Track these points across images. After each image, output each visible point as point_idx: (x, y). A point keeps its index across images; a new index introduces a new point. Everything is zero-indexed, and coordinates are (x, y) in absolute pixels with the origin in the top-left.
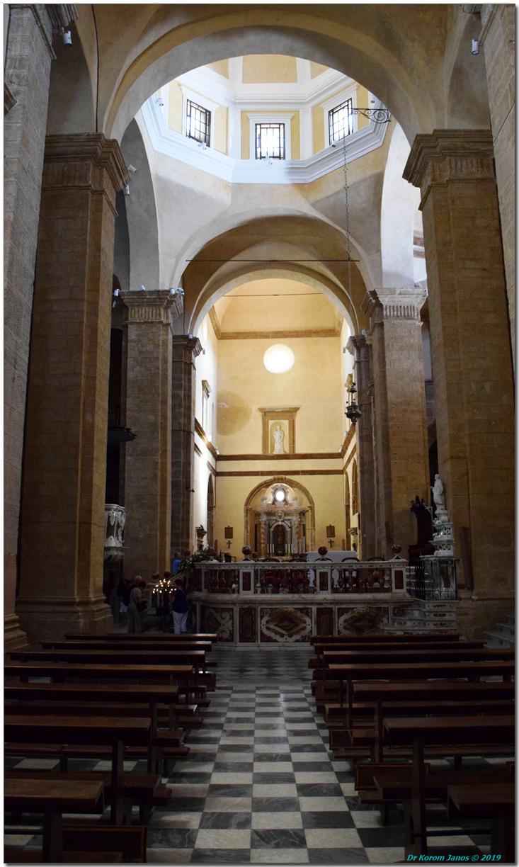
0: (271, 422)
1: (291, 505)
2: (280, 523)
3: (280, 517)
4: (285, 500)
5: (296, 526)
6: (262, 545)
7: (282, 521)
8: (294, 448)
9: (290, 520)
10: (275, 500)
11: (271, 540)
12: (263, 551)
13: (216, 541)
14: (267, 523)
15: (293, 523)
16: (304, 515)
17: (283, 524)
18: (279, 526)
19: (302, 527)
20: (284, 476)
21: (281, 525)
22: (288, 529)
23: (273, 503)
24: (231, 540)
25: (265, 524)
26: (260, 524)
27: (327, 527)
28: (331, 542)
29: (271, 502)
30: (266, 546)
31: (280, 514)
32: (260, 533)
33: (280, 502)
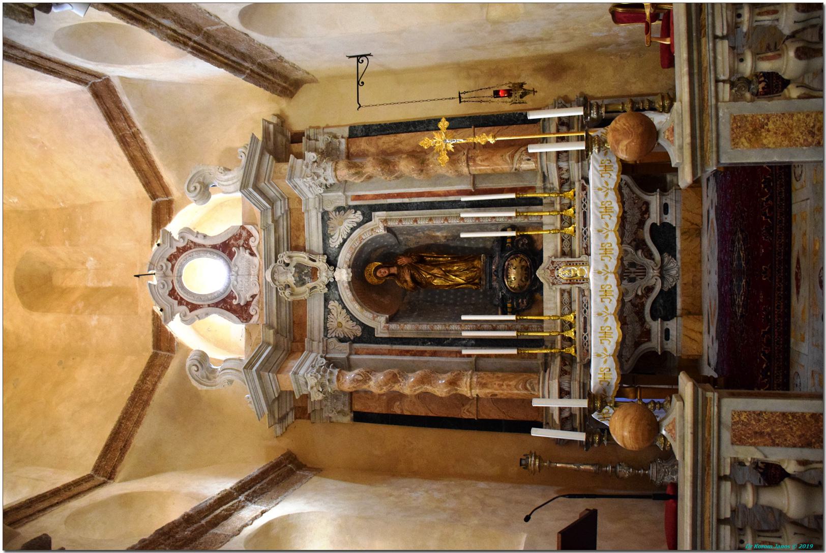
2: (343, 275)
3: (305, 274)
5: (344, 173)
6: (464, 389)
7: (332, 263)
9: (325, 217)
11: (438, 328)
12: (511, 389)
14: (340, 352)
15: (338, 198)
17: (345, 257)
18: (359, 283)
19: (363, 144)
21: (359, 266)
22: (377, 226)
23: (242, 312)
25: (345, 365)
30: (477, 365)
31: (290, 279)
32: (424, 397)
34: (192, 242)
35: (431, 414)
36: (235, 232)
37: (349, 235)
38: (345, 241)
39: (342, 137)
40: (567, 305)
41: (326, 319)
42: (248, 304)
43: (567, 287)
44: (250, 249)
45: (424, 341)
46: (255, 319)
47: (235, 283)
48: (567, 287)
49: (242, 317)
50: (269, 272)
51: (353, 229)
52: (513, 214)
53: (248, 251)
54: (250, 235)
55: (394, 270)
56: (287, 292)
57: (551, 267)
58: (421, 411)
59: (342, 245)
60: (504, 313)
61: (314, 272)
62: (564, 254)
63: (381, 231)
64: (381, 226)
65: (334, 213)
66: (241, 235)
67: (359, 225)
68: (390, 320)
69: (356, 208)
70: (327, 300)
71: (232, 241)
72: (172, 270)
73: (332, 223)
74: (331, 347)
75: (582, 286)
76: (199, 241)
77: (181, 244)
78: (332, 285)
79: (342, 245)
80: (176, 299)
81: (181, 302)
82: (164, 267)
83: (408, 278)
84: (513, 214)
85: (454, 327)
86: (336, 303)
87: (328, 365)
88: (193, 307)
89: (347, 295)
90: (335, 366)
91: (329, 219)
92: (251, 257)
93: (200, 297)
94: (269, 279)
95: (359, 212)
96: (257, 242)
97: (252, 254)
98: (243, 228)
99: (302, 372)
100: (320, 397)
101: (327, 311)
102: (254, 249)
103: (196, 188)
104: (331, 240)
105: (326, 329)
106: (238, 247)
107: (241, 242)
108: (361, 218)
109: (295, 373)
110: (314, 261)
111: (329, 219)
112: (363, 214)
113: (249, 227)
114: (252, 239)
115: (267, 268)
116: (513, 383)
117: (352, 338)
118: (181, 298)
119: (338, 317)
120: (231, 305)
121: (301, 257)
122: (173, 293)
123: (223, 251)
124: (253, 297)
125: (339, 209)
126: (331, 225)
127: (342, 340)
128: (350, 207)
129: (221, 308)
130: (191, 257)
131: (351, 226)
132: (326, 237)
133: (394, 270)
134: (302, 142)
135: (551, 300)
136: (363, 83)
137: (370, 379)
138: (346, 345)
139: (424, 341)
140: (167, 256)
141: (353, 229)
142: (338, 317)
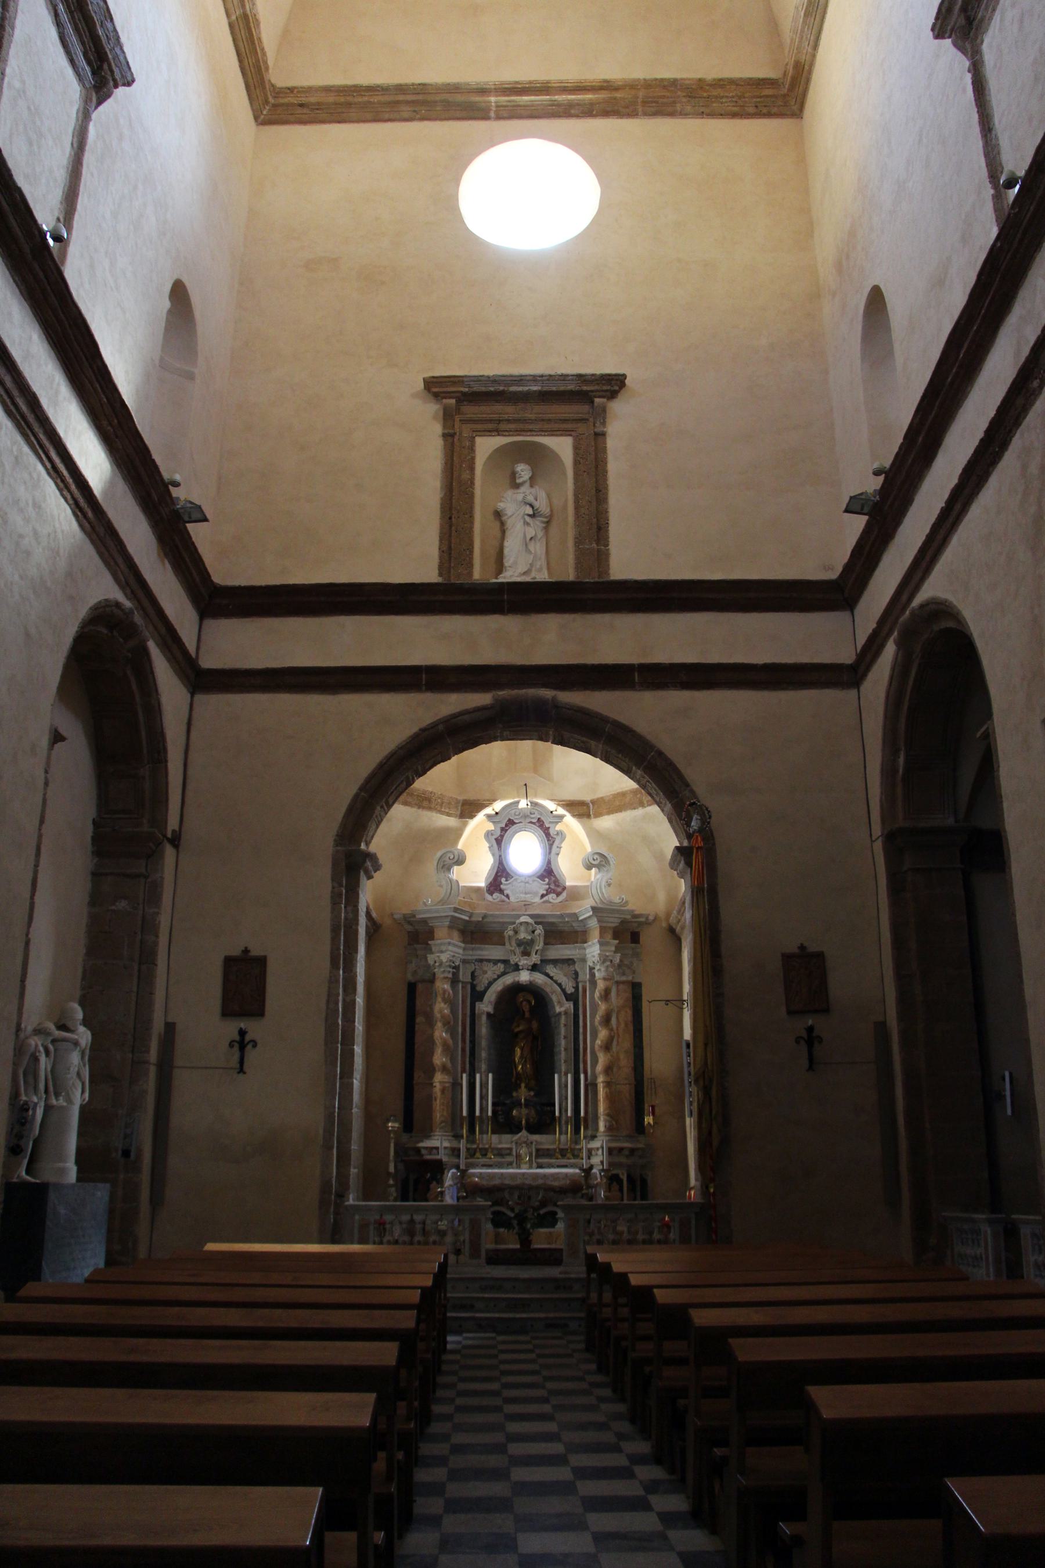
0: (486, 446)
1: (576, 894)
2: (524, 977)
3: (526, 947)
4: (548, 873)
5: (601, 985)
8: (602, 557)
9: (570, 962)
10: (501, 874)
12: (439, 1111)
13: (170, 1028)
14: (464, 976)
15: (584, 976)
16: (635, 938)
17: (539, 978)
18: (517, 988)
20: (547, 693)
22: (561, 1007)
24: (254, 1028)
25: (454, 981)
26: (432, 980)
27: (787, 958)
28: (811, 1039)
29: (482, 884)
30: (456, 1085)
31: (523, 935)
33: (527, 879)
34: (553, 842)
35: (416, 1046)
36: (561, 881)
37: (556, 982)
38: (551, 978)
39: (633, 977)
40: (500, 1153)
41: (489, 961)
42: (501, 891)
43: (514, 1153)
44: (547, 895)
45: (473, 1042)
46: (489, 897)
47: (519, 881)
48: (514, 1153)
49: (491, 887)
50: (529, 920)
51: (560, 985)
52: (569, 1114)
53: (545, 892)
54: (558, 894)
55: (527, 1015)
56: (511, 933)
57: (529, 1142)
58: (419, 1039)
59: (547, 975)
60: (494, 1104)
61: (526, 953)
62: (538, 1150)
63: (558, 1009)
64: (563, 1009)
65: (573, 969)
66: (558, 886)
67: (564, 991)
68: (489, 1015)
69: (577, 988)
70: (505, 962)
71: (553, 879)
72: (531, 822)
73: (565, 966)
74: (468, 966)
75: (514, 1164)
76: (554, 847)
77: (551, 831)
78: (517, 968)
79: (547, 975)
80: (506, 825)
81: (504, 830)
82: (533, 816)
83: (521, 1028)
84: (569, 1114)
85: (484, 1067)
86: (502, 970)
87: (454, 968)
88: (499, 841)
89: (509, 980)
90: (454, 974)
91: (569, 965)
92: (540, 895)
93: (507, 848)
94: (523, 919)
95: (573, 990)
96: (551, 900)
97: (543, 896)
98: (564, 888)
99: (450, 948)
100: (431, 961)
101: (496, 962)
102: (545, 899)
103: (594, 860)
104: (552, 966)
105: (481, 961)
106: (548, 884)
107: (552, 886)
108: (569, 992)
109: (449, 943)
110: (536, 954)
111: (569, 965)
112: (572, 994)
113: (564, 894)
114: (554, 896)
115: (531, 916)
116: (445, 1114)
117: (475, 983)
118: (507, 830)
119: (492, 971)
120: (501, 876)
121: (539, 945)
122: (511, 823)
123: (545, 870)
124: (508, 896)
125: (576, 974)
126: (564, 966)
127: (473, 974)
128: (577, 983)
129: (498, 867)
130: (541, 842)
131: (563, 984)
132: (555, 962)
133: (527, 1015)
134: (632, 943)
135: (503, 1141)
136: (667, 1004)
137: (445, 1003)
138: (469, 980)
139: (473, 1042)
140: (542, 818)
141: (560, 985)
142: (492, 971)
